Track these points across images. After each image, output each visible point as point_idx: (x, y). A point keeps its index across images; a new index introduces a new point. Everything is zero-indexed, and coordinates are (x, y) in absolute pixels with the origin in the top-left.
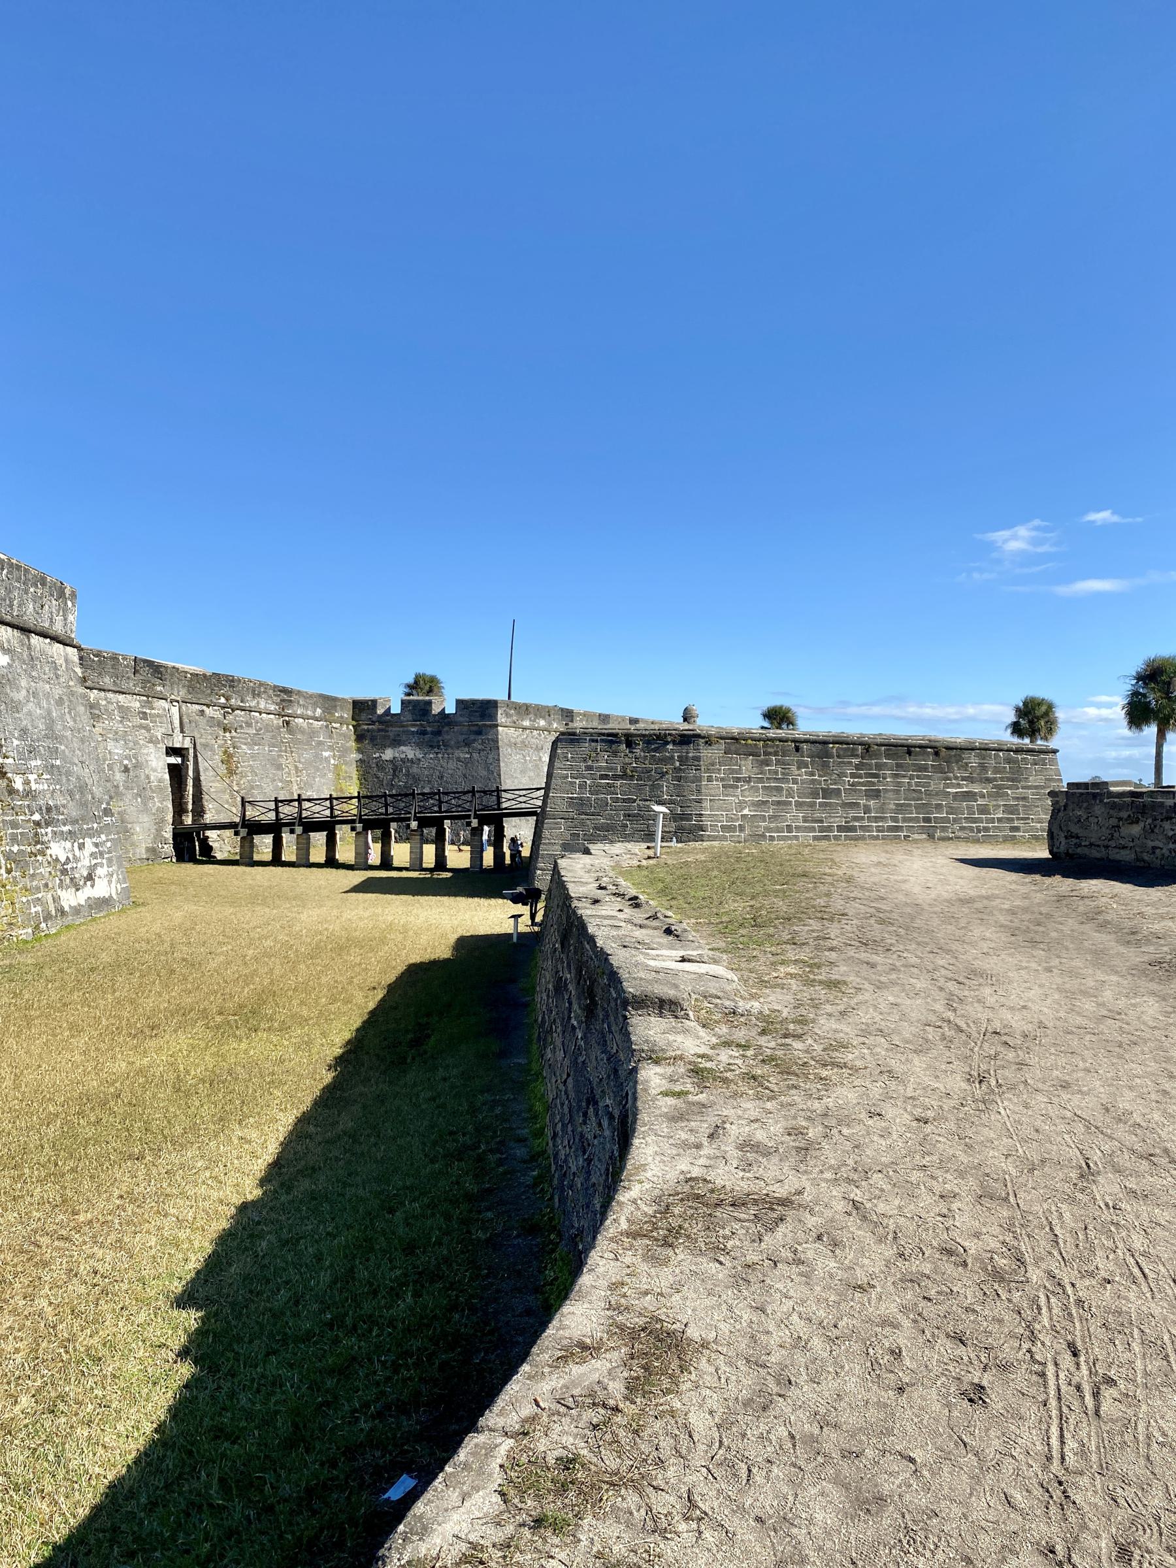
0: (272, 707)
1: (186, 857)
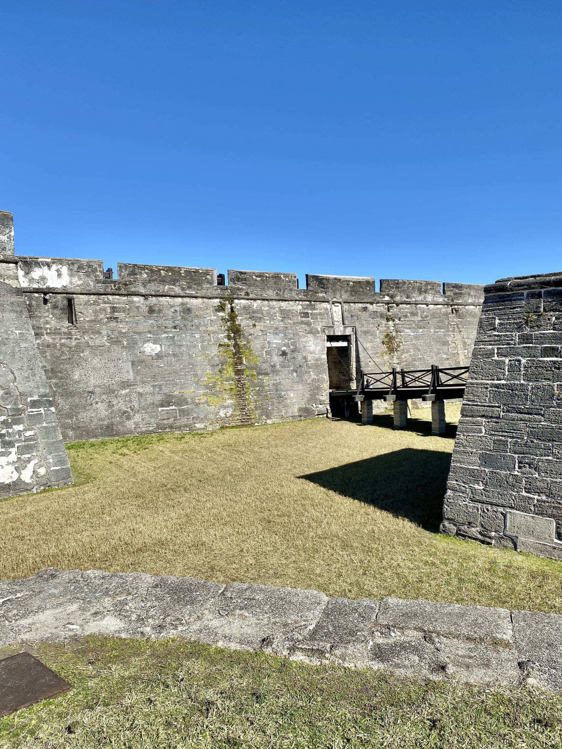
0: (441, 300)
1: (347, 414)
